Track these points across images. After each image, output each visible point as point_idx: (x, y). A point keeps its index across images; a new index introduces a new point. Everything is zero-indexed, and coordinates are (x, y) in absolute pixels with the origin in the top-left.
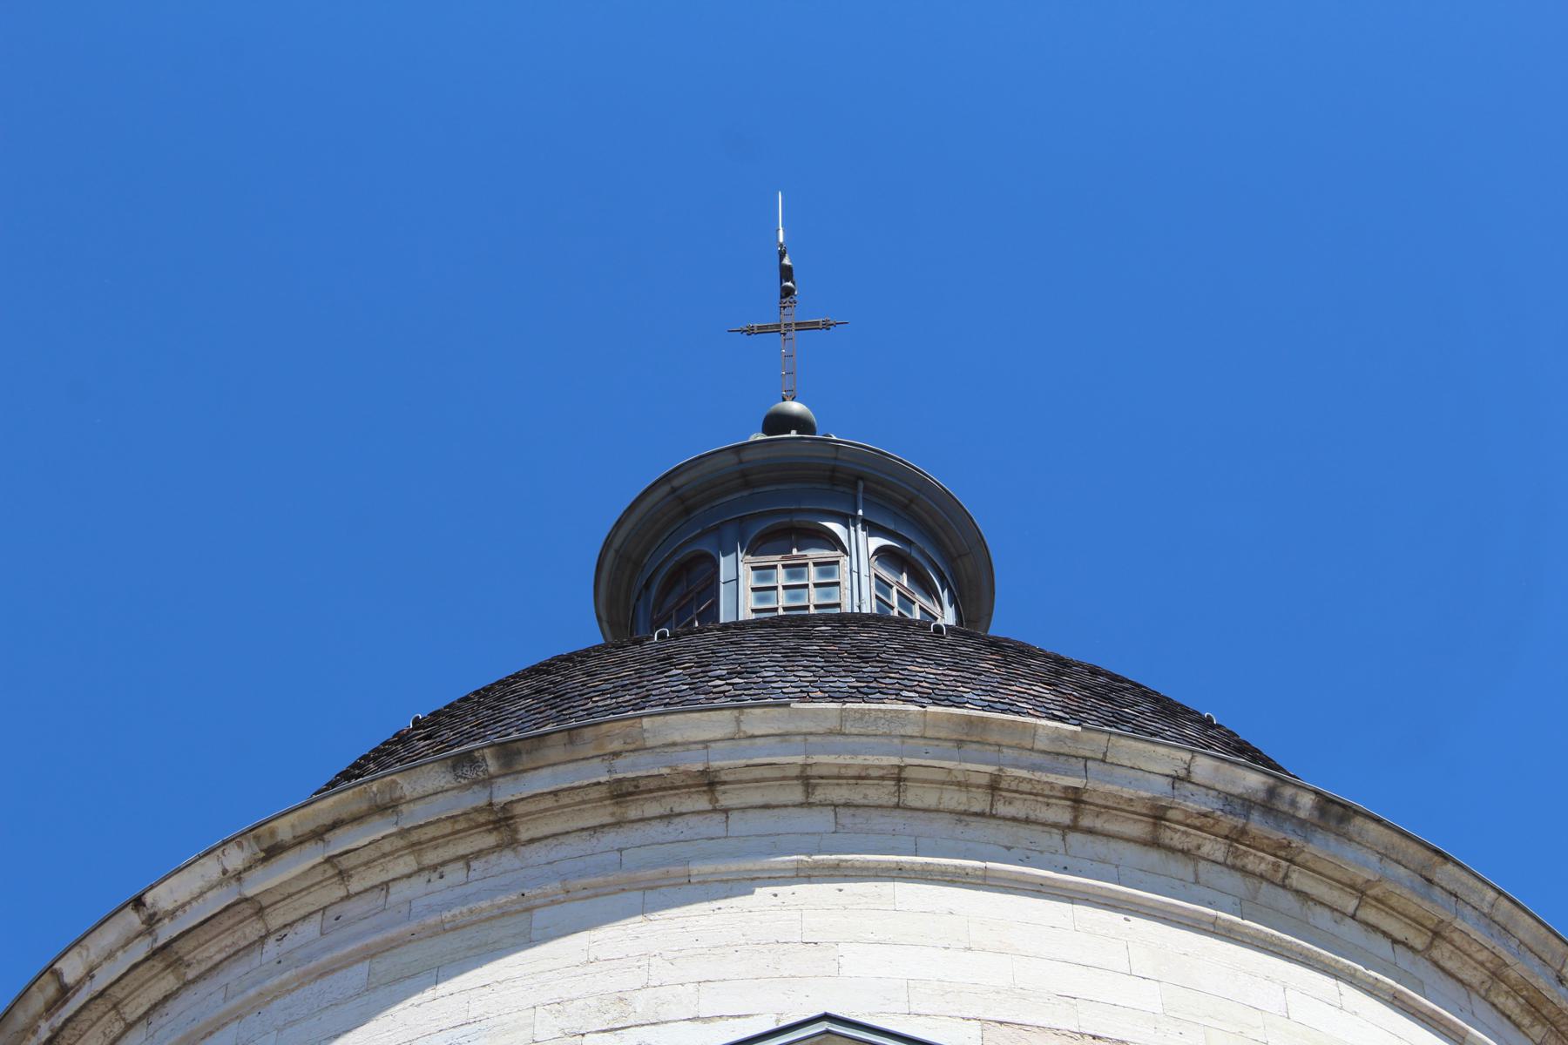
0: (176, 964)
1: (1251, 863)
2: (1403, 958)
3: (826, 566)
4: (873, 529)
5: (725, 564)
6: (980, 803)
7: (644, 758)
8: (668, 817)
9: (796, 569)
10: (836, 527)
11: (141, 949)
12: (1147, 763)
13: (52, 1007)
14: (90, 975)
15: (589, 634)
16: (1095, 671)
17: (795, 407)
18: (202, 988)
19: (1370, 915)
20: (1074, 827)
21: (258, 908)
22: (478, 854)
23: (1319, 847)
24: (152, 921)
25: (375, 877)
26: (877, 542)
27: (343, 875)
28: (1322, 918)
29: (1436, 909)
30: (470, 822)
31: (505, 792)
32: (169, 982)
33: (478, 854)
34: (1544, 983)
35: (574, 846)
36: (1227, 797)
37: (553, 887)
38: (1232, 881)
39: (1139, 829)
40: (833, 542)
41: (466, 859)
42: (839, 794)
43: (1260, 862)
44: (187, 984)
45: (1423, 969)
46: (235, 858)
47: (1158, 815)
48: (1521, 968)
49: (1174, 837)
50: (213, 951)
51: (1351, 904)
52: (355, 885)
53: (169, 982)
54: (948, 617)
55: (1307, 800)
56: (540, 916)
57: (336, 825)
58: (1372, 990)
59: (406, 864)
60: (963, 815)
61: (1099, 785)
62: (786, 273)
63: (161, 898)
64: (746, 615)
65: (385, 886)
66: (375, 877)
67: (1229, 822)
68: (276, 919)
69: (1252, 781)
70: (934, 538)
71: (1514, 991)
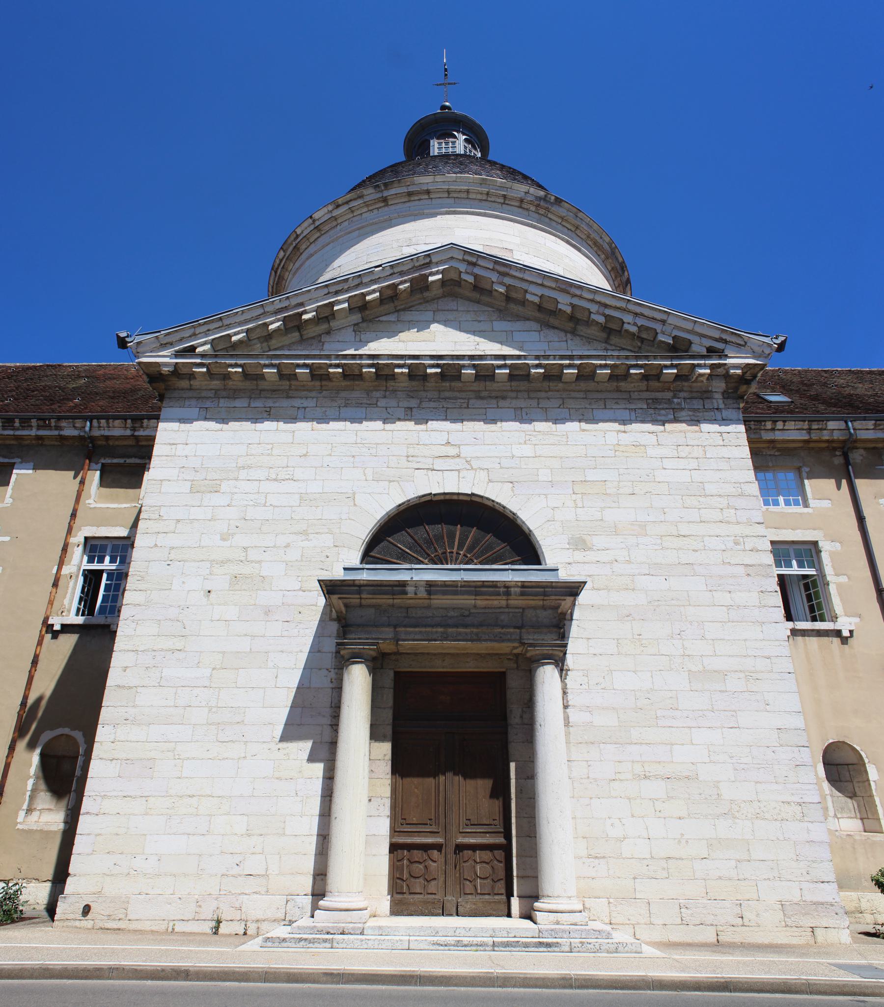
0: (320, 230)
2: (570, 233)
3: (454, 143)
4: (464, 134)
6: (484, 197)
8: (419, 200)
9: (447, 143)
11: (312, 227)
12: (520, 189)
15: (404, 159)
16: (510, 168)
17: (447, 104)
19: (564, 223)
20: (504, 203)
21: (335, 218)
23: (554, 208)
24: (314, 221)
25: (359, 212)
26: (464, 137)
27: (353, 212)
28: (554, 224)
29: (578, 222)
31: (386, 194)
32: (318, 234)
34: (598, 238)
35: (400, 206)
36: (536, 197)
38: (536, 215)
39: (517, 204)
40: (455, 137)
41: (378, 208)
42: (455, 195)
43: (542, 211)
45: (574, 235)
46: (330, 208)
47: (522, 201)
48: (593, 235)
49: (525, 206)
50: (327, 228)
51: (560, 221)
53: (318, 234)
54: (479, 155)
55: (553, 198)
57: (351, 200)
58: (563, 239)
59: (365, 209)
60: (481, 200)
61: (510, 194)
62: (446, 70)
63: (316, 216)
64: (436, 154)
66: (359, 212)
68: (339, 221)
69: (542, 193)
70: (477, 137)
71: (592, 240)
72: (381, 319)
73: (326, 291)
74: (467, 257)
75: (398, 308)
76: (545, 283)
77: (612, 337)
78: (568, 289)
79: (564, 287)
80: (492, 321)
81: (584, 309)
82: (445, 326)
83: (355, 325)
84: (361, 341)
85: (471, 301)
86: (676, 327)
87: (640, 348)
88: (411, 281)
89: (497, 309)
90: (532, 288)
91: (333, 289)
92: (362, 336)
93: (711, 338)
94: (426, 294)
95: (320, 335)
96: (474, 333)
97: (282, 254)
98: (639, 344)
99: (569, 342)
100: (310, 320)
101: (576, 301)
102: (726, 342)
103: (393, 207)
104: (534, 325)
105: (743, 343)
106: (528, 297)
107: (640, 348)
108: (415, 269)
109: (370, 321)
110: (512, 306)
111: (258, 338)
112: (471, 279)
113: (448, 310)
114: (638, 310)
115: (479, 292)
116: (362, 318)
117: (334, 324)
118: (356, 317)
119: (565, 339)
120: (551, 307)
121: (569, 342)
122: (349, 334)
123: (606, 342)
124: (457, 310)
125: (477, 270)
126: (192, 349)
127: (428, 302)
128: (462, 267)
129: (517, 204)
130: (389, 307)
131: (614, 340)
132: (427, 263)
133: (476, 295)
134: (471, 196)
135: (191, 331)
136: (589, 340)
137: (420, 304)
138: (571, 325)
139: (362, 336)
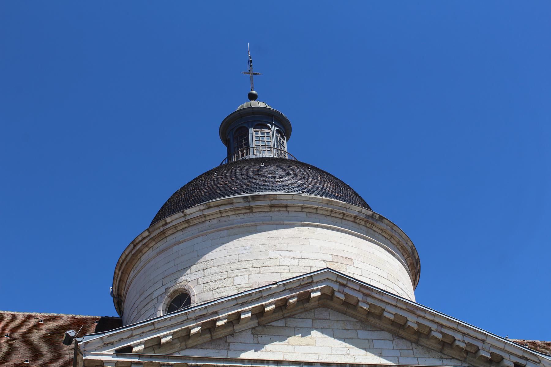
1: (368, 225)
5: (250, 130)
6: (329, 214)
7: (276, 201)
10: (269, 125)
13: (163, 226)
14: (172, 222)
18: (193, 228)
22: (246, 213)
24: (185, 215)
25: (227, 214)
30: (245, 208)
32: (186, 225)
33: (246, 213)
35: (263, 214)
37: (261, 222)
42: (307, 210)
44: (190, 226)
49: (357, 221)
50: (196, 222)
52: (223, 215)
56: (259, 227)
59: (233, 213)
61: (347, 212)
65: (229, 216)
66: (227, 214)
67: (366, 219)
72: (273, 324)
73: (235, 302)
74: (339, 280)
75: (285, 315)
76: (398, 305)
77: (445, 348)
78: (415, 311)
79: (412, 309)
80: (356, 330)
81: (426, 326)
82: (323, 333)
83: (253, 328)
84: (258, 343)
85: (339, 312)
86: (492, 346)
87: (465, 358)
88: (298, 296)
89: (360, 320)
90: (388, 308)
91: (240, 301)
92: (260, 339)
93: (516, 355)
94: (307, 305)
95: (226, 337)
96: (344, 340)
97: (147, 233)
98: (465, 355)
99: (415, 350)
100: (222, 325)
101: (421, 321)
102: (527, 359)
103: (257, 215)
104: (388, 336)
105: (538, 361)
106: (386, 314)
107: (465, 358)
108: (301, 287)
109: (264, 326)
110: (371, 319)
111: (178, 338)
112: (342, 297)
113: (323, 319)
114: (466, 331)
115: (348, 307)
116: (258, 323)
117: (237, 328)
118: (254, 323)
119: (411, 348)
120: (401, 322)
121: (415, 350)
122: (248, 337)
123: (441, 352)
124: (329, 319)
125: (347, 290)
126: (130, 349)
127: (307, 311)
128: (336, 287)
129: (352, 219)
130: (279, 314)
131: (447, 351)
132: (310, 283)
133: (344, 308)
134: (319, 212)
135: (129, 334)
136: (429, 350)
137: (302, 312)
138: (415, 337)
139: (260, 339)
